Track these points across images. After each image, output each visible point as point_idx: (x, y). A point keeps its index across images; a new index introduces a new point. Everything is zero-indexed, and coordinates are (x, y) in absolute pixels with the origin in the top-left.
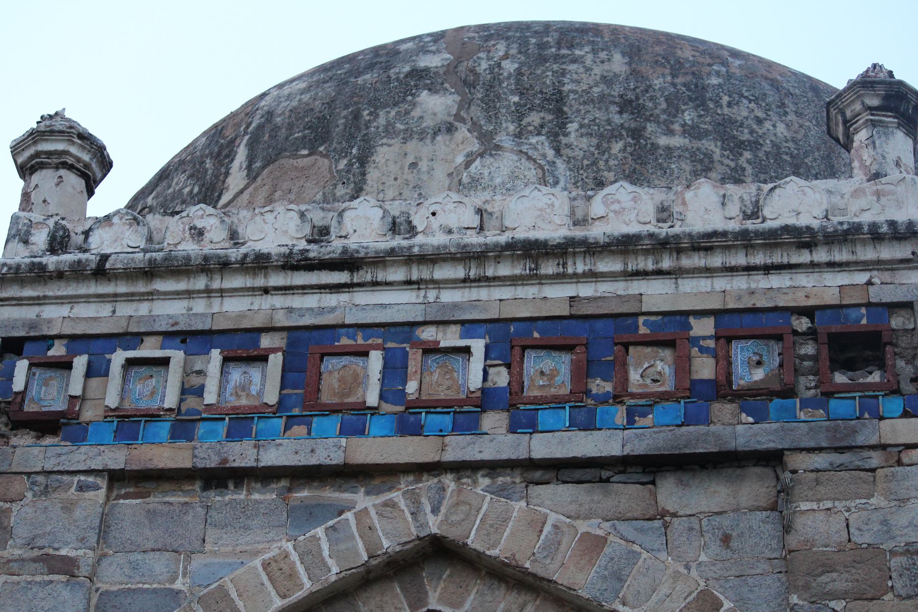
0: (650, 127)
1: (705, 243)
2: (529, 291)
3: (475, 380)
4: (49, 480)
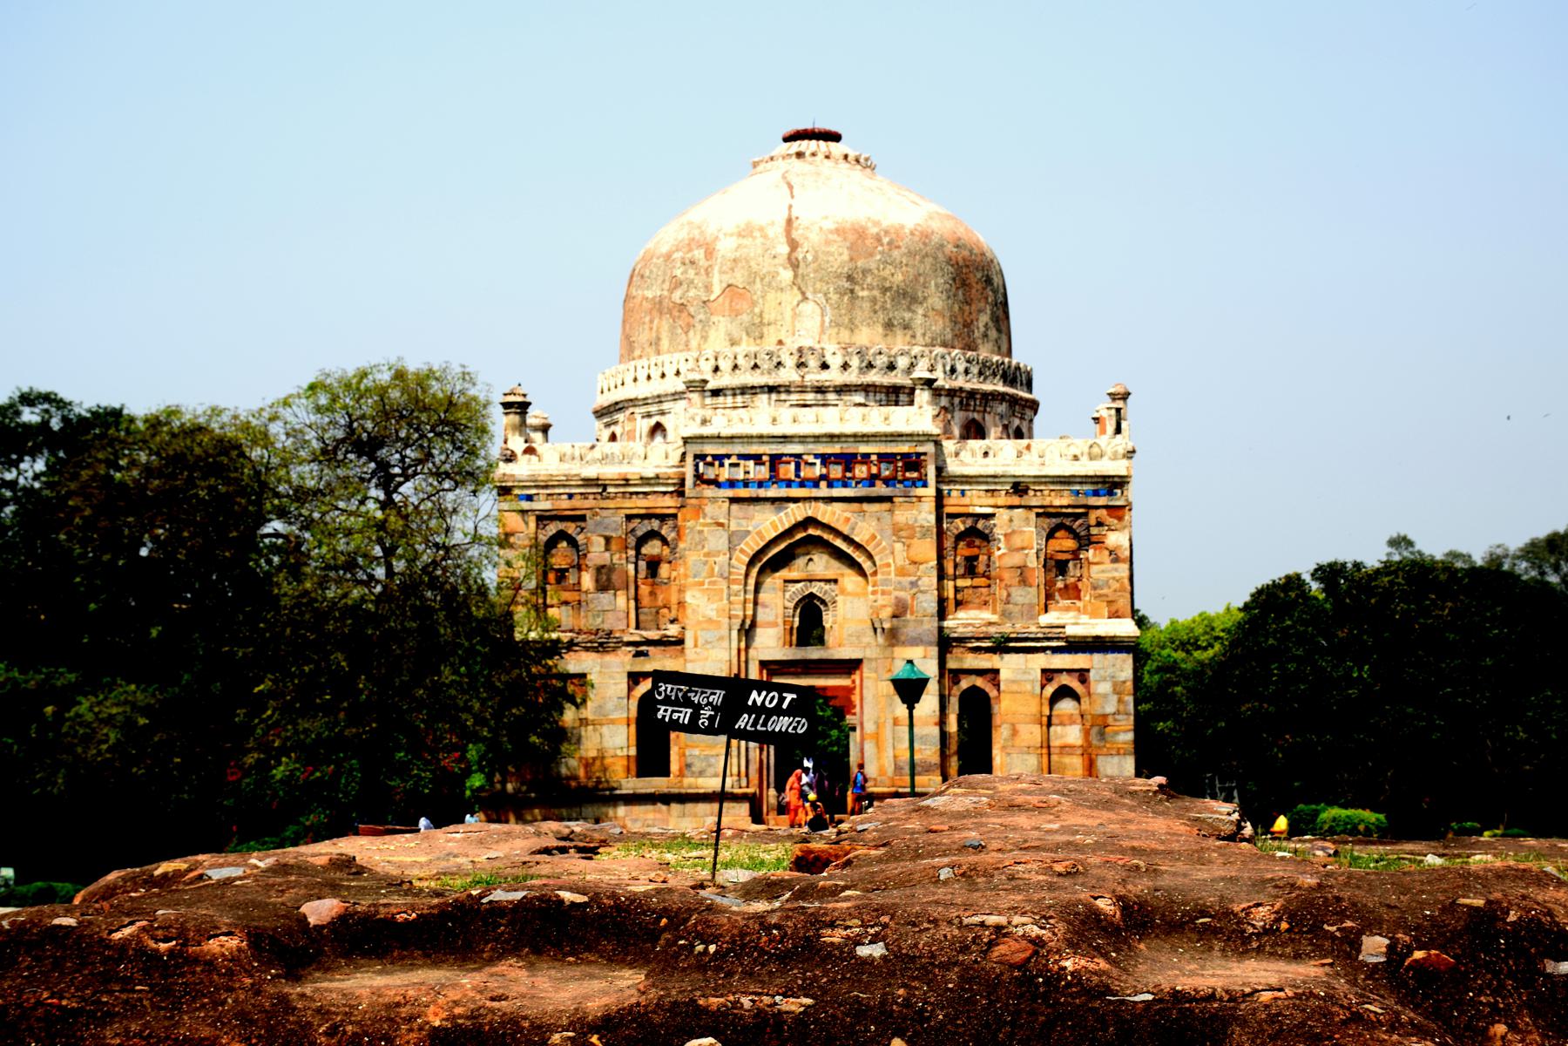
0: (857, 288)
4: (714, 500)
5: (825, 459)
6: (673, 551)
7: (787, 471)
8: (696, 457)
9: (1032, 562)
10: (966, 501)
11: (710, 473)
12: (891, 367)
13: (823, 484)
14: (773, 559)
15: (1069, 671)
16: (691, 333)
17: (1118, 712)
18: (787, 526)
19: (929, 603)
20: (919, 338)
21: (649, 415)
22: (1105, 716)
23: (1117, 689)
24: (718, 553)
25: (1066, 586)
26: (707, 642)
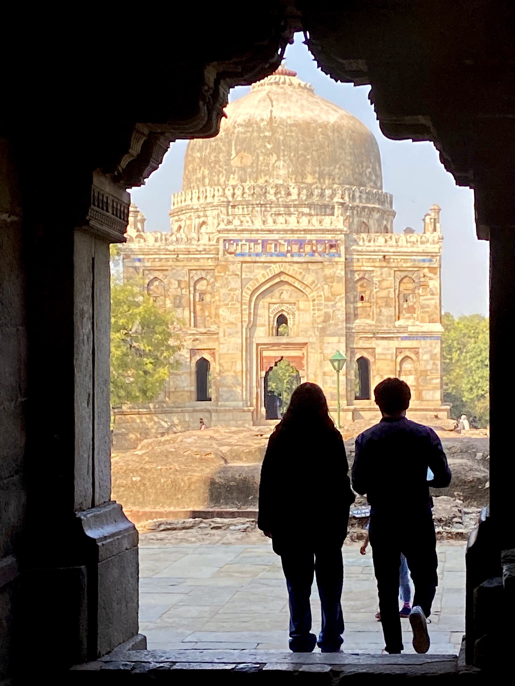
1: (314, 230)
2: (292, 235)
3: (286, 249)
4: (233, 263)
5: (290, 242)
6: (213, 288)
7: (270, 248)
8: (224, 240)
9: (392, 295)
10: (360, 264)
11: (232, 250)
12: (322, 195)
13: (289, 255)
14: (262, 292)
15: (410, 349)
16: (221, 176)
17: (433, 369)
18: (270, 276)
19: (341, 315)
20: (337, 181)
21: (199, 217)
22: (426, 371)
23: (433, 357)
24: (236, 289)
25: (408, 307)
26: (230, 334)
